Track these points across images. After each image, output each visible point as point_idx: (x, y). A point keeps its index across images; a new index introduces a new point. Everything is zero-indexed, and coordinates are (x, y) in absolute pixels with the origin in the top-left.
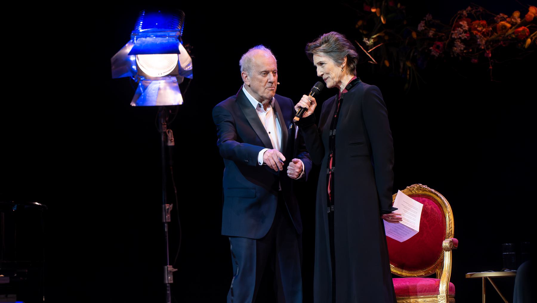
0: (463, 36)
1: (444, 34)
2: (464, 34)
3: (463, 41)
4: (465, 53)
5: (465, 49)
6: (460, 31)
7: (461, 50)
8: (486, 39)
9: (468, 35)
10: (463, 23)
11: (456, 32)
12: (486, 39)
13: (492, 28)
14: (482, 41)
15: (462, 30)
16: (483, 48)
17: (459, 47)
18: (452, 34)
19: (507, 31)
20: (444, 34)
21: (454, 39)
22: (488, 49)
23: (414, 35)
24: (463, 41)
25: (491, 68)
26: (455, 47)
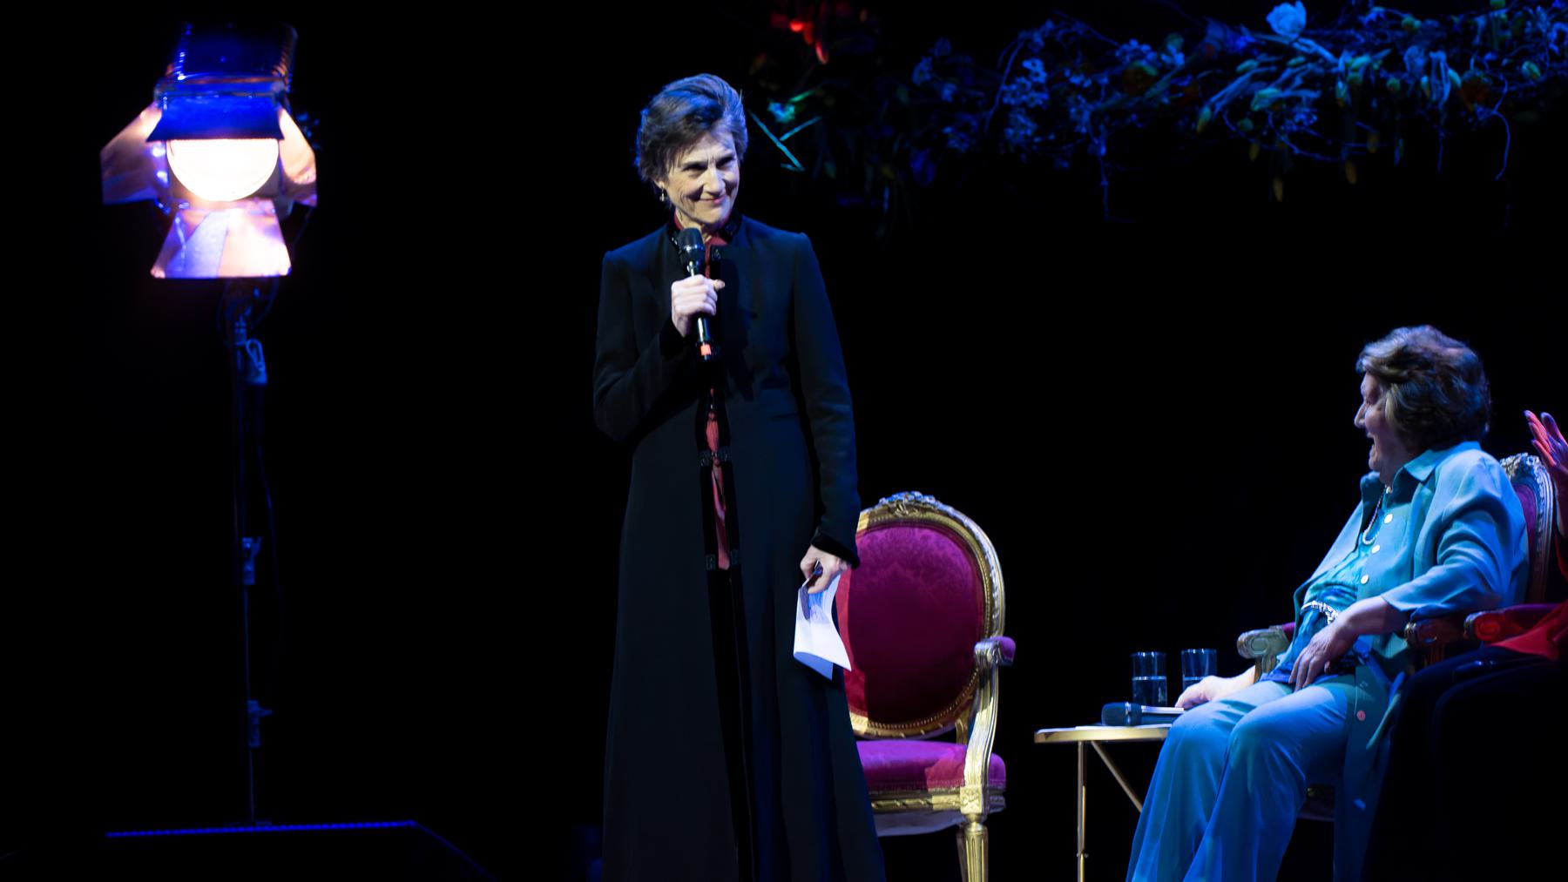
0: (1032, 100)
1: (981, 94)
2: (1035, 95)
3: (1033, 113)
4: (1037, 144)
5: (1037, 133)
6: (1024, 85)
7: (1026, 136)
8: (1091, 107)
9: (1046, 96)
10: (1034, 65)
11: (1014, 87)
12: (1091, 107)
13: (1110, 79)
14: (1080, 113)
15: (1029, 84)
16: (1084, 130)
17: (1022, 129)
18: (1003, 94)
19: (1148, 88)
20: (981, 94)
21: (1009, 108)
22: (1097, 133)
23: (903, 95)
24: (1033, 113)
25: (1105, 183)
26: (1012, 127)
